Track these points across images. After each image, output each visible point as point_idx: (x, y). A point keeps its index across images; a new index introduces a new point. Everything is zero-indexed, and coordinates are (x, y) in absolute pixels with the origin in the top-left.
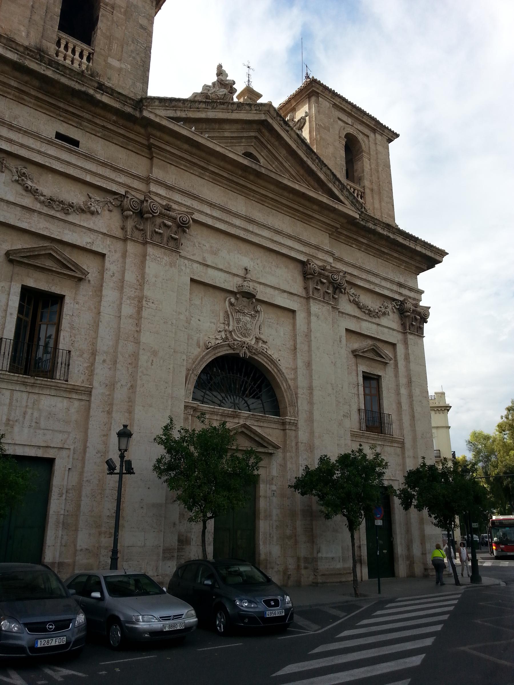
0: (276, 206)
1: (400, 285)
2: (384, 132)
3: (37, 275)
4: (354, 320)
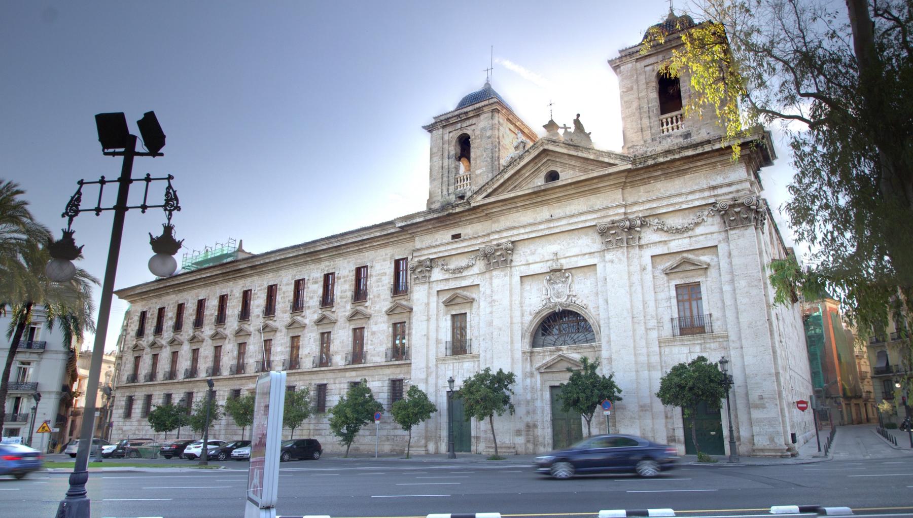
0: (569, 197)
1: (714, 188)
3: (456, 307)
4: (661, 245)
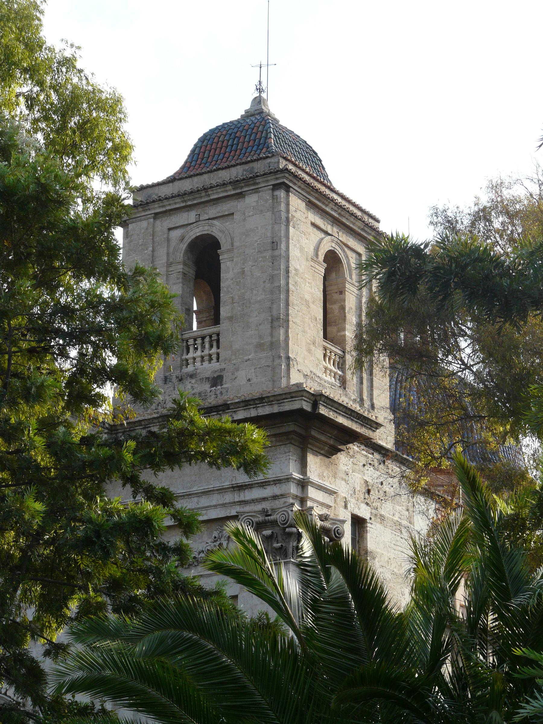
2: (258, 184)
